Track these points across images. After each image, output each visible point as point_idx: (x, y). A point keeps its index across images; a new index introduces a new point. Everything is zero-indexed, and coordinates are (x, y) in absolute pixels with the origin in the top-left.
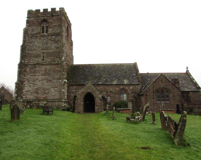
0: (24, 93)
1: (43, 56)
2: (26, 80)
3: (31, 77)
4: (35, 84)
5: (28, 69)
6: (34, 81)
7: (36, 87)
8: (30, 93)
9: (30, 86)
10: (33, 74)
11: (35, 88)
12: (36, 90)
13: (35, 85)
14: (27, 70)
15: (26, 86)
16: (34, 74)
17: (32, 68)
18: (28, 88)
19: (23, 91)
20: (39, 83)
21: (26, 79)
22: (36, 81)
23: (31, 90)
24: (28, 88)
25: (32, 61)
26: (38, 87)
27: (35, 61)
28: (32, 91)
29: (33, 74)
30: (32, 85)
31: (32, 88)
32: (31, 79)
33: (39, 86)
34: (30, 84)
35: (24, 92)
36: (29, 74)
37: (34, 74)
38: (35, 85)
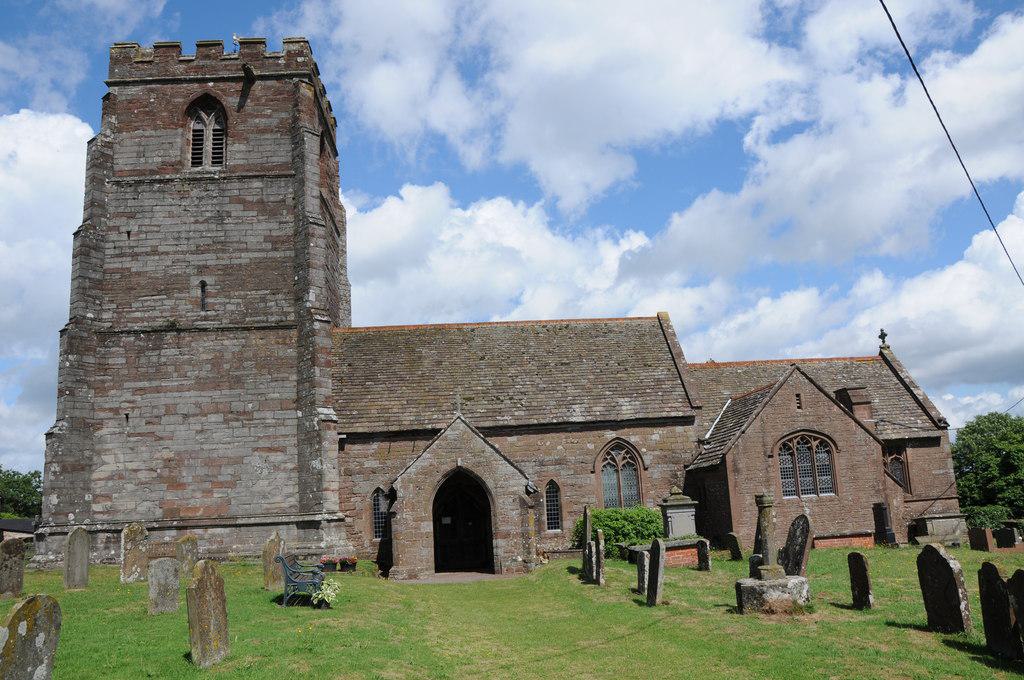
0: (99, 488)
1: (203, 285)
6: (156, 420)
7: (167, 454)
9: (132, 449)
11: (158, 455)
15: (109, 446)
16: (155, 384)
17: (141, 351)
18: (121, 457)
19: (95, 476)
23: (136, 471)
25: (138, 314)
26: (178, 453)
28: (143, 476)
32: (137, 412)
35: (102, 483)
36: (126, 385)
37: (155, 384)
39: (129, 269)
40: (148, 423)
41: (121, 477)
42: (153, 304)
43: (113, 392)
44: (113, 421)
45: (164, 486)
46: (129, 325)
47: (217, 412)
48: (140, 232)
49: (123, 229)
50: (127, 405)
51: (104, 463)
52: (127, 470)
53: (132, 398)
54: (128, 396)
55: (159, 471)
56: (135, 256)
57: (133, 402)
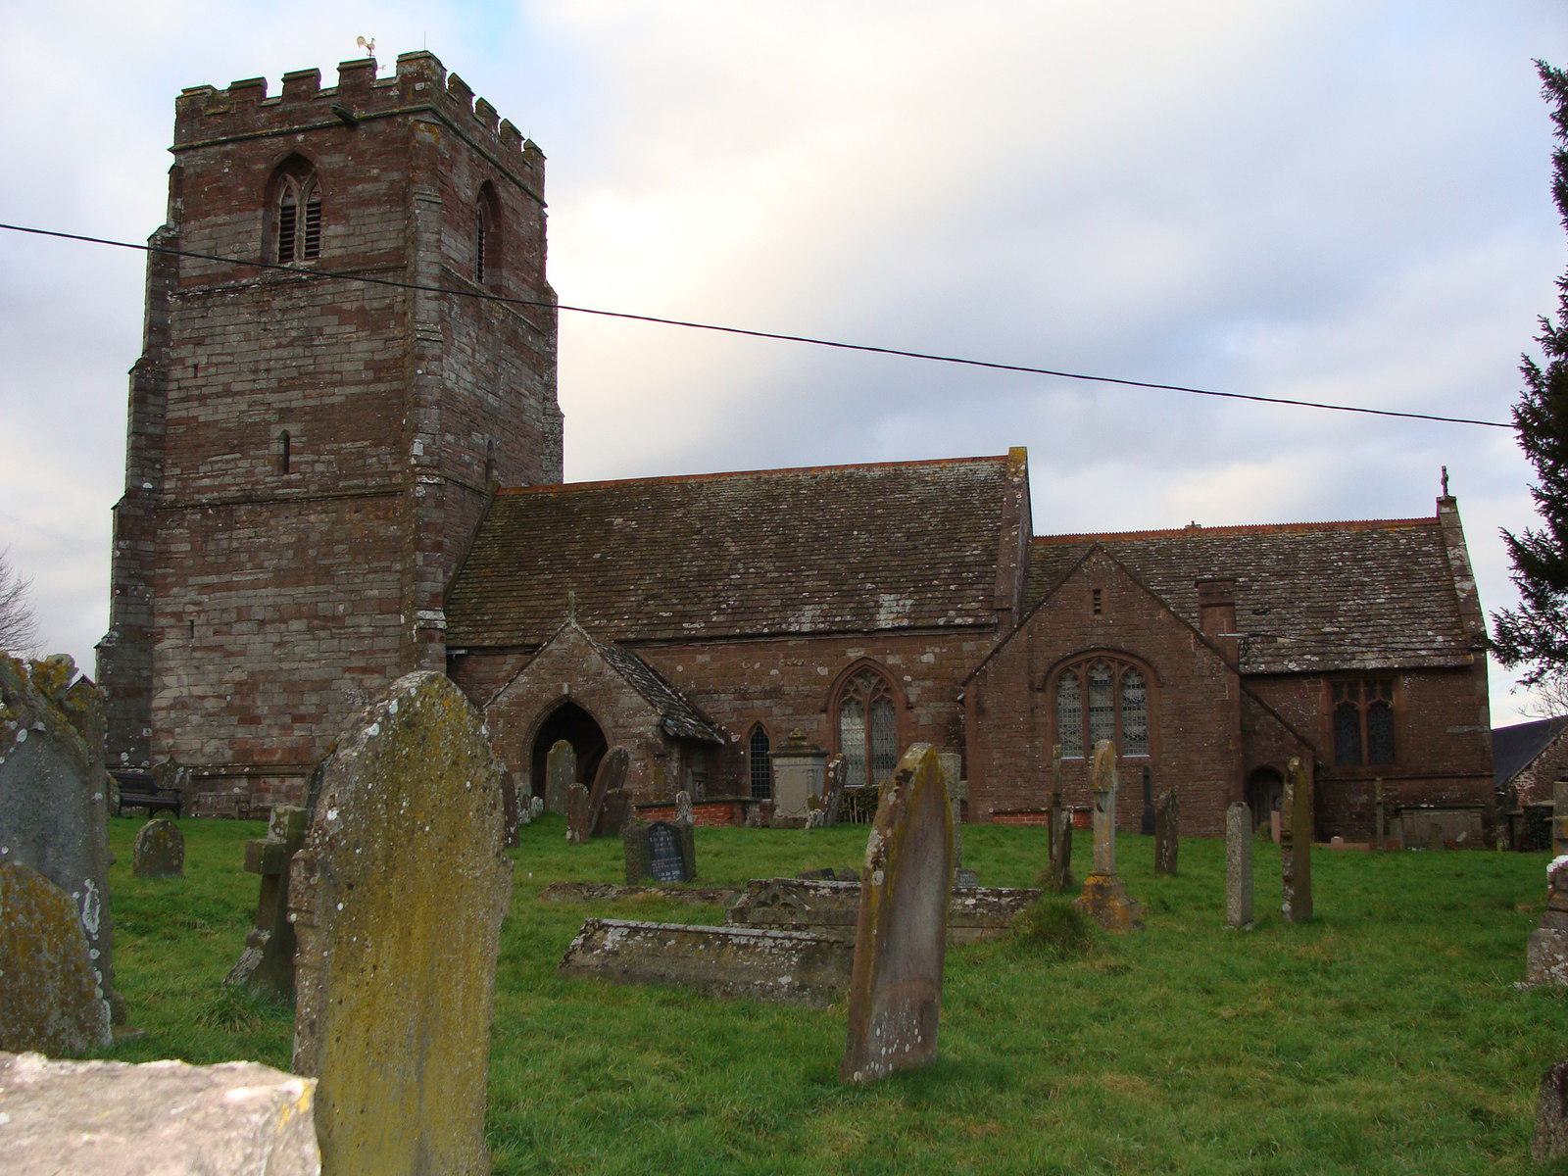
0: (160, 719)
2: (172, 621)
3: (205, 598)
5: (183, 540)
6: (225, 629)
7: (239, 676)
9: (197, 668)
10: (213, 579)
11: (227, 677)
13: (231, 654)
14: (173, 548)
15: (172, 663)
16: (225, 578)
17: (208, 534)
18: (185, 679)
20: (258, 639)
21: (173, 614)
22: (236, 627)
23: (202, 698)
24: (185, 679)
25: (206, 482)
26: (252, 674)
27: (228, 480)
28: (210, 704)
29: (213, 579)
31: (213, 677)
35: (163, 713)
36: (191, 580)
37: (225, 578)
38: (231, 654)
39: (196, 418)
40: (215, 633)
41: (185, 706)
42: (224, 466)
43: (175, 590)
44: (175, 630)
45: (235, 719)
46: (196, 497)
47: (299, 618)
48: (209, 365)
49: (190, 362)
50: (192, 608)
51: (165, 687)
52: (191, 696)
53: (199, 598)
54: (192, 595)
55: (229, 698)
56: (202, 399)
57: (200, 603)
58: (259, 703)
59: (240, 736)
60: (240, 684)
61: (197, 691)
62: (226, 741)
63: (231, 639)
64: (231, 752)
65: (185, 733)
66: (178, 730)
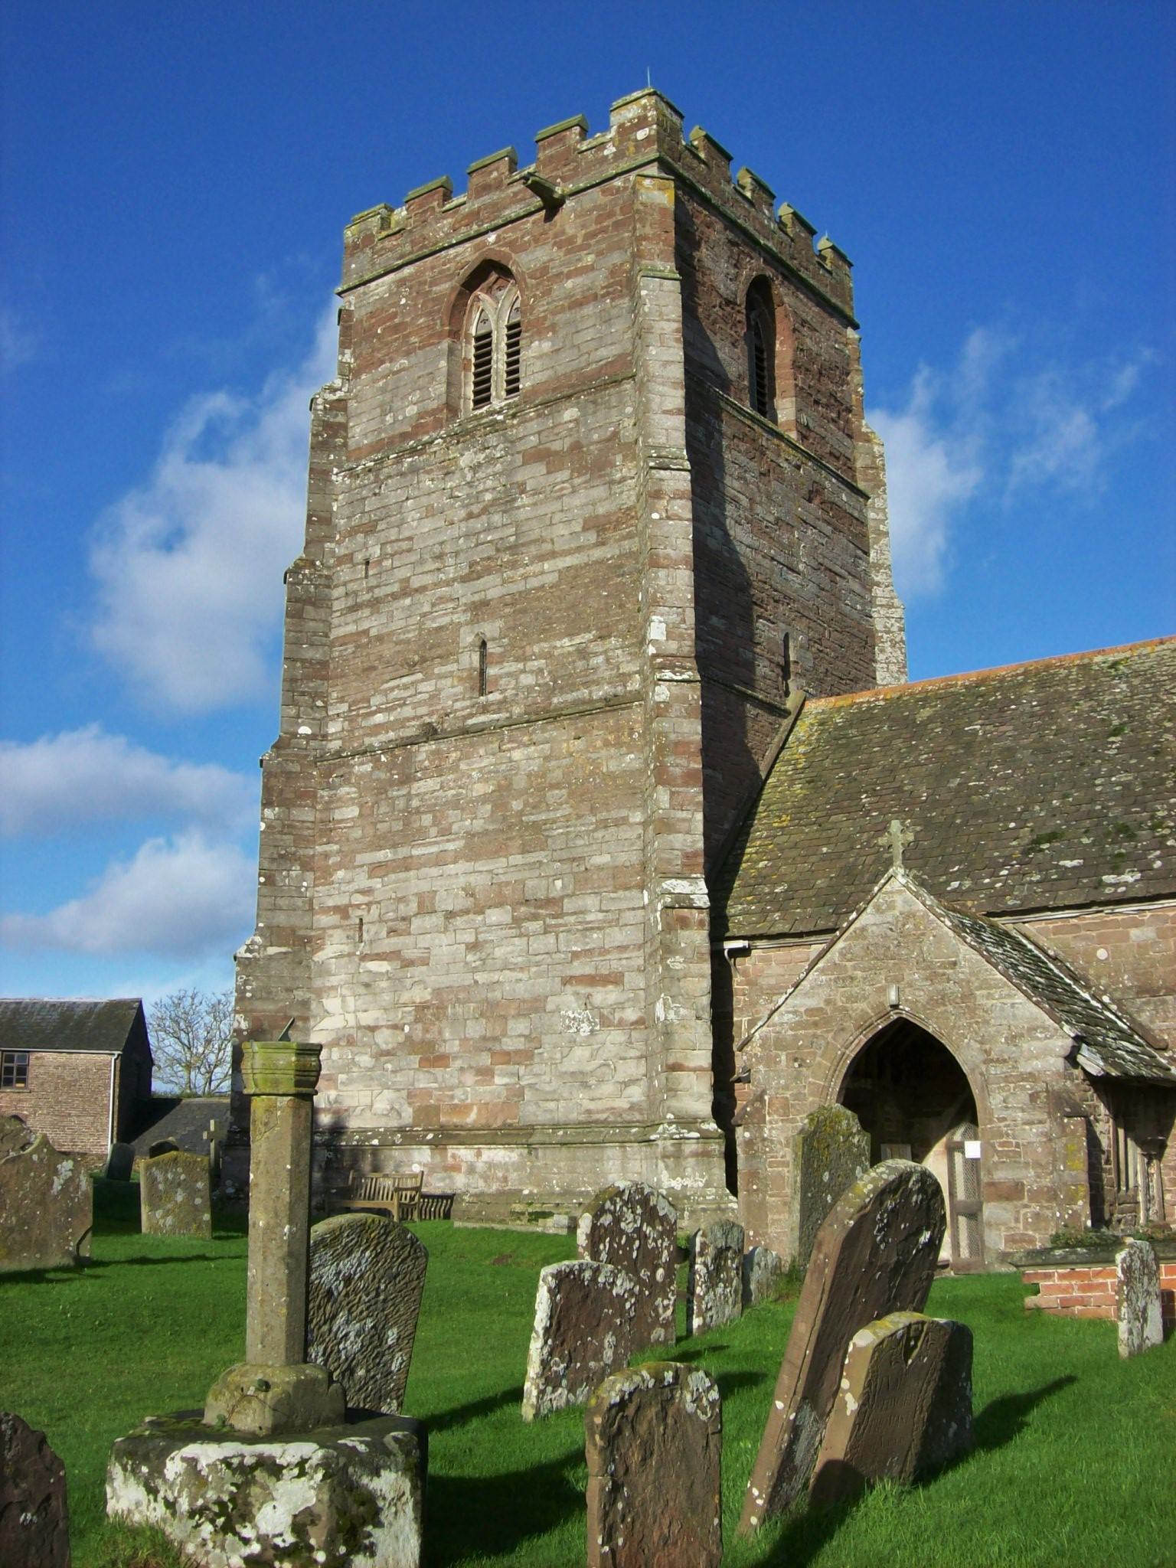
4: (410, 954)
7: (420, 995)
8: (365, 1060)
9: (367, 985)
12: (417, 1021)
13: (409, 963)
18: (351, 1001)
20: (444, 939)
21: (336, 909)
23: (372, 1029)
26: (437, 992)
28: (385, 1039)
30: (382, 967)
31: (387, 997)
33: (444, 981)
34: (364, 958)
38: (409, 963)
40: (392, 932)
41: (351, 1042)
45: (415, 1059)
50: (359, 899)
55: (407, 1029)
58: (447, 1035)
59: (421, 1086)
60: (422, 1008)
61: (367, 1019)
62: (404, 1093)
63: (408, 940)
64: (411, 1110)
65: (350, 1081)
66: (342, 1077)
